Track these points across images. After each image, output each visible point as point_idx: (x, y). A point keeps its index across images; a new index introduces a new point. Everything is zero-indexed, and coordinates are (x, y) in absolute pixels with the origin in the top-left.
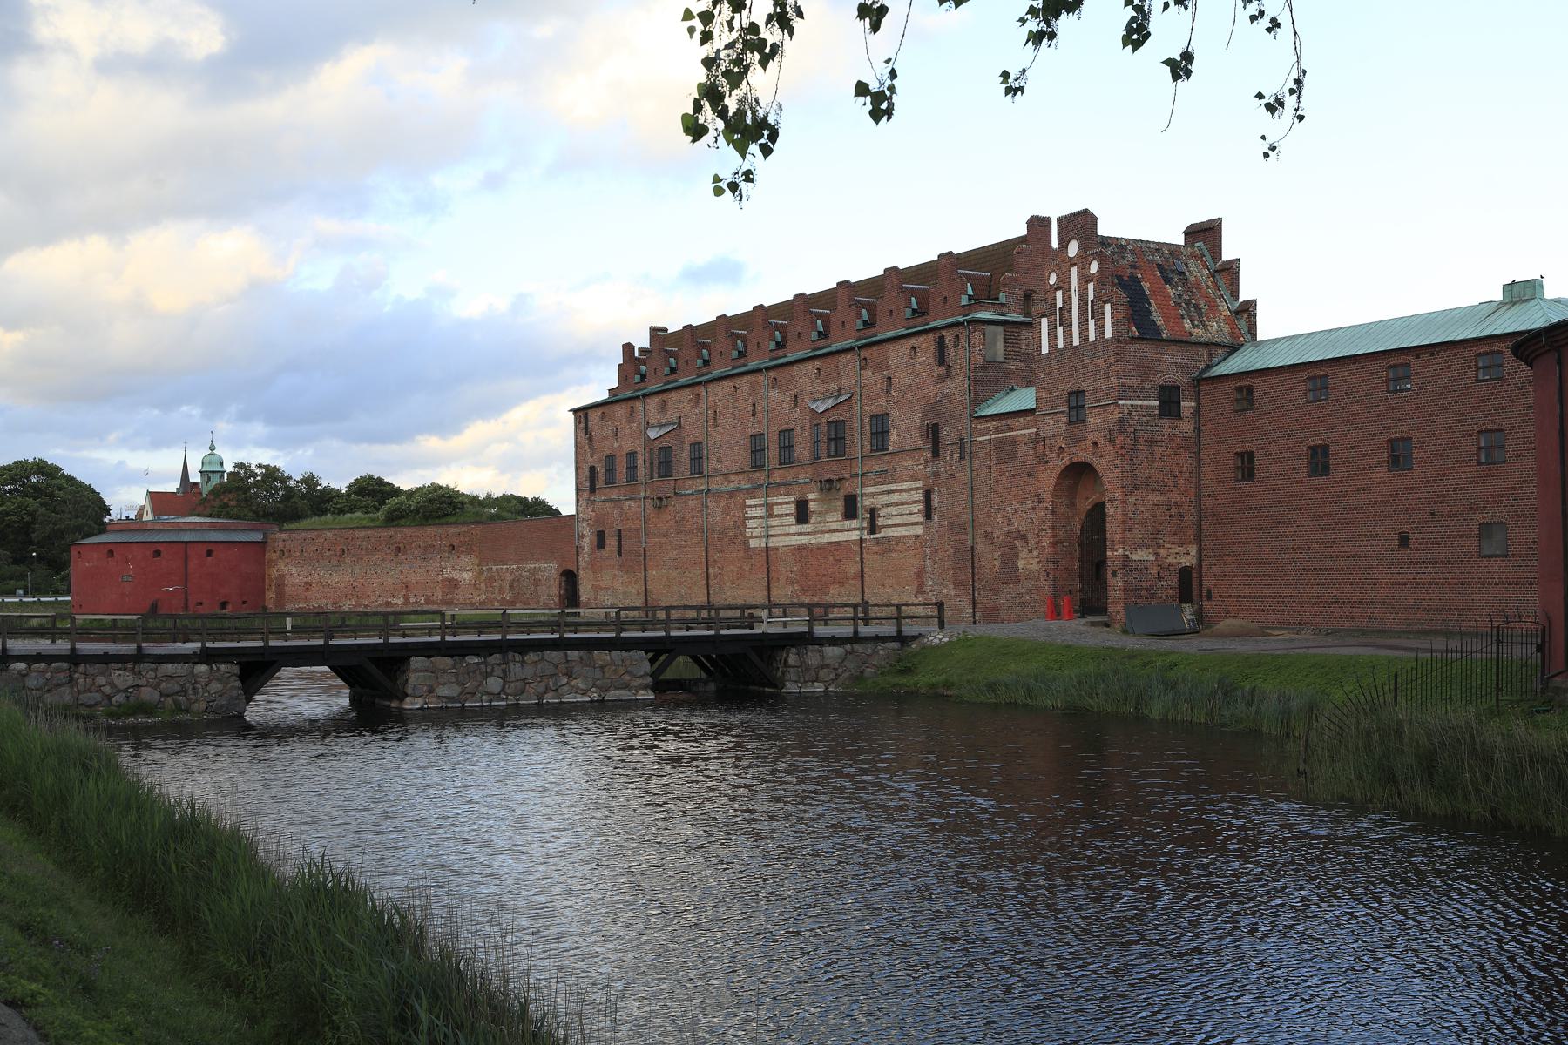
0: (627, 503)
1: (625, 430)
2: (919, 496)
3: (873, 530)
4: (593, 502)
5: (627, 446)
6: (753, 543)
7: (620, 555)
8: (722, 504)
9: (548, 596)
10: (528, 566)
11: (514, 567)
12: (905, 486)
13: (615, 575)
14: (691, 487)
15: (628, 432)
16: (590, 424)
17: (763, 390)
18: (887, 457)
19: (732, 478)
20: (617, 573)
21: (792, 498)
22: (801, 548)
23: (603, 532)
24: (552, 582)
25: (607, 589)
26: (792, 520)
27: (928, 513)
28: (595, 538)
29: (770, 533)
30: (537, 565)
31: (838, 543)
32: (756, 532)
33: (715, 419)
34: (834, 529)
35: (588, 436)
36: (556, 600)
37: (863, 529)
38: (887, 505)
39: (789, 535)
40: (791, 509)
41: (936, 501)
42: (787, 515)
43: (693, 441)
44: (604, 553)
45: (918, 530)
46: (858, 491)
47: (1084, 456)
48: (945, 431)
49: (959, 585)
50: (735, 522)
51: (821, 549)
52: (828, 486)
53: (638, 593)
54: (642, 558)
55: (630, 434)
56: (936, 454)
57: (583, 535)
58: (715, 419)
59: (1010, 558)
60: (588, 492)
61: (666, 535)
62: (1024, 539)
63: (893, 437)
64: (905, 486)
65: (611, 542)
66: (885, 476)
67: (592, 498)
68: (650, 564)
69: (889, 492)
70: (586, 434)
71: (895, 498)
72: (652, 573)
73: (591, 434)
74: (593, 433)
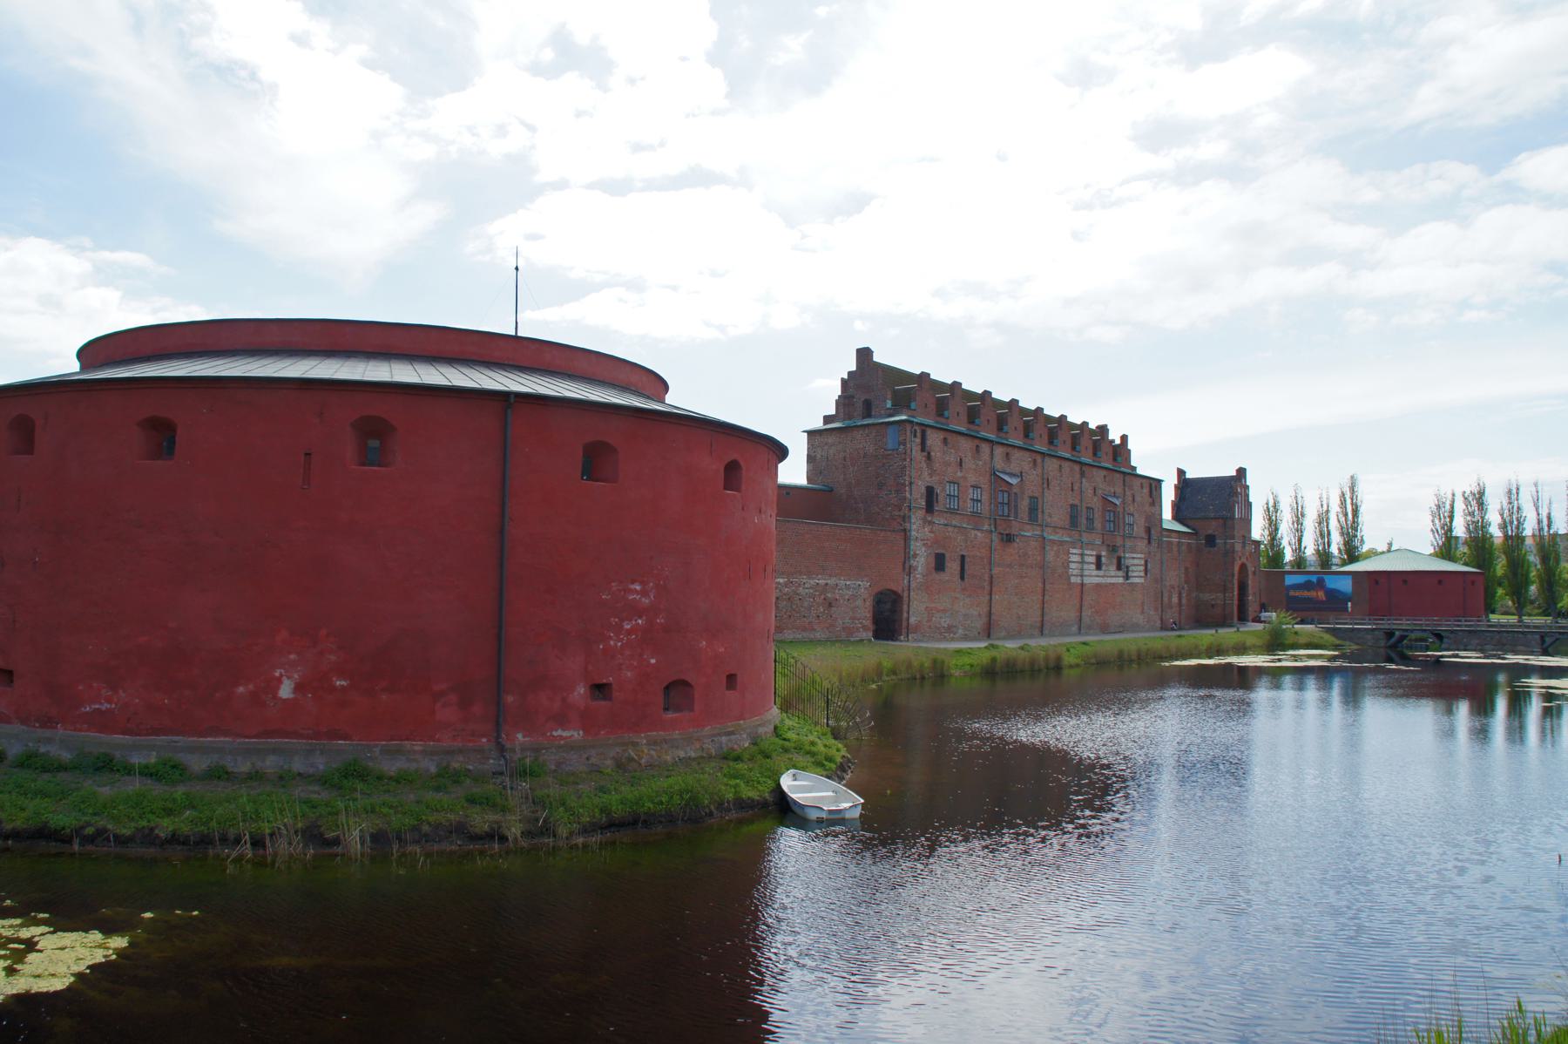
0: (973, 531)
1: (969, 462)
2: (1143, 562)
3: (1127, 577)
4: (931, 523)
5: (972, 479)
6: (1073, 580)
7: (962, 578)
8: (1055, 549)
9: (853, 618)
10: (812, 582)
11: (781, 581)
12: (1139, 556)
13: (956, 598)
14: (1028, 531)
15: (974, 466)
16: (929, 443)
17: (1078, 476)
18: (1132, 539)
19: (1058, 530)
20: (958, 596)
21: (1094, 553)
22: (1098, 585)
23: (943, 555)
24: (859, 602)
25: (944, 611)
26: (1093, 567)
27: (1146, 571)
28: (932, 560)
29: (1086, 573)
30: (831, 582)
31: (1113, 584)
32: (1075, 572)
33: (1048, 485)
34: (1114, 577)
35: (925, 454)
36: (869, 623)
37: (1123, 577)
38: (1134, 565)
39: (1093, 577)
40: (1092, 559)
41: (1149, 565)
42: (1092, 563)
43: (1031, 494)
44: (944, 576)
45: (1142, 580)
46: (1122, 555)
47: (1244, 560)
48: (1153, 532)
49: (1156, 609)
50: (1063, 563)
51: (1107, 586)
52: (1113, 549)
53: (980, 615)
54: (986, 584)
55: (975, 470)
56: (1149, 542)
57: (915, 555)
58: (1048, 485)
59: (1170, 598)
60: (924, 511)
61: (1010, 566)
62: (1174, 588)
63: (1135, 528)
64: (1139, 556)
65: (953, 566)
66: (1133, 550)
67: (929, 519)
68: (994, 589)
69: (1134, 558)
70: (923, 450)
71: (1136, 562)
72: (996, 597)
73: (929, 453)
74: (933, 454)
